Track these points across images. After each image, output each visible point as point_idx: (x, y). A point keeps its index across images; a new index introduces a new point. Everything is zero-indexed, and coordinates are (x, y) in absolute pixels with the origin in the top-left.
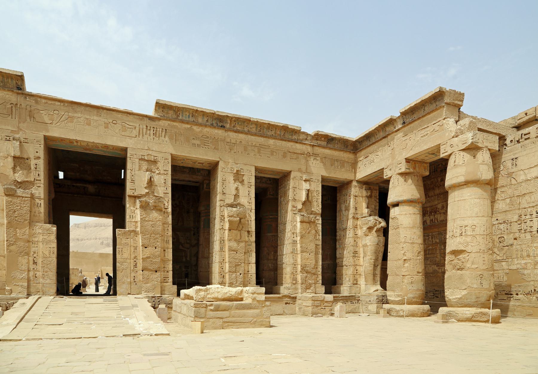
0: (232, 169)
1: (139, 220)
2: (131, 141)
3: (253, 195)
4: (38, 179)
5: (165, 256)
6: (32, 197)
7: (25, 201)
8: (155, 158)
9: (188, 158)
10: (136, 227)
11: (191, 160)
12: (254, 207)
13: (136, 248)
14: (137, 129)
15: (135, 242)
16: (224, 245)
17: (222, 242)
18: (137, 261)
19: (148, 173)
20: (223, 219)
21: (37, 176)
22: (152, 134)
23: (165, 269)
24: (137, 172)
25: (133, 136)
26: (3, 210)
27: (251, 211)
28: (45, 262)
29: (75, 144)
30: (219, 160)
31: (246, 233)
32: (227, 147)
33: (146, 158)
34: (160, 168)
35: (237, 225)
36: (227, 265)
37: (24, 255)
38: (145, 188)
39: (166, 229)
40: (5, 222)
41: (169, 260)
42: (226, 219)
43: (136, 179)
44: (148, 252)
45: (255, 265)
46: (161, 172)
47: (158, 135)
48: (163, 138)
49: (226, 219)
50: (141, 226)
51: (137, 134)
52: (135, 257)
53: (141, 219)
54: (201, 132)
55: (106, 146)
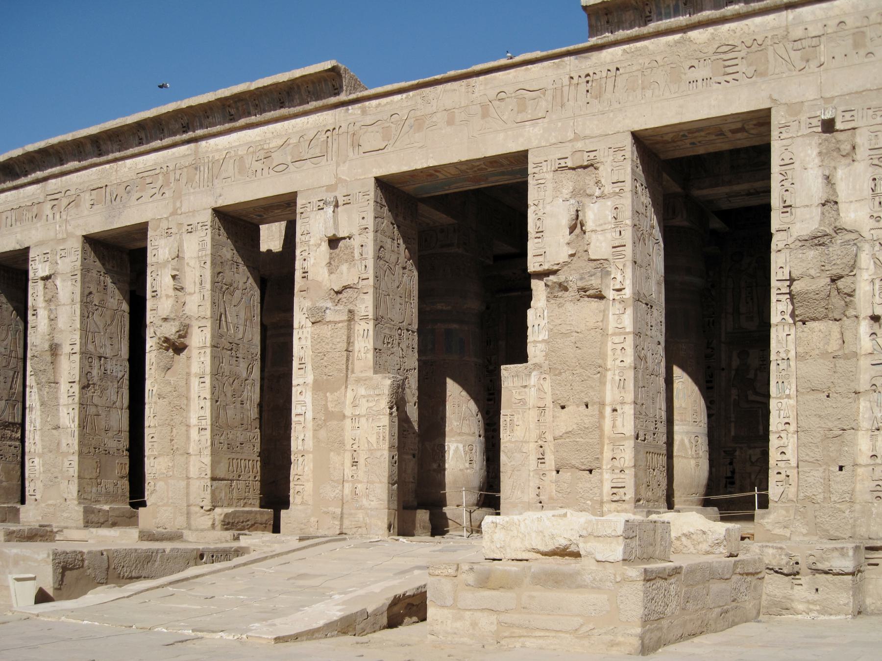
4: (365, 276)
8: (592, 155)
13: (542, 409)
32: (796, 56)
34: (603, 181)
39: (620, 347)
46: (606, 192)
54: (713, 38)
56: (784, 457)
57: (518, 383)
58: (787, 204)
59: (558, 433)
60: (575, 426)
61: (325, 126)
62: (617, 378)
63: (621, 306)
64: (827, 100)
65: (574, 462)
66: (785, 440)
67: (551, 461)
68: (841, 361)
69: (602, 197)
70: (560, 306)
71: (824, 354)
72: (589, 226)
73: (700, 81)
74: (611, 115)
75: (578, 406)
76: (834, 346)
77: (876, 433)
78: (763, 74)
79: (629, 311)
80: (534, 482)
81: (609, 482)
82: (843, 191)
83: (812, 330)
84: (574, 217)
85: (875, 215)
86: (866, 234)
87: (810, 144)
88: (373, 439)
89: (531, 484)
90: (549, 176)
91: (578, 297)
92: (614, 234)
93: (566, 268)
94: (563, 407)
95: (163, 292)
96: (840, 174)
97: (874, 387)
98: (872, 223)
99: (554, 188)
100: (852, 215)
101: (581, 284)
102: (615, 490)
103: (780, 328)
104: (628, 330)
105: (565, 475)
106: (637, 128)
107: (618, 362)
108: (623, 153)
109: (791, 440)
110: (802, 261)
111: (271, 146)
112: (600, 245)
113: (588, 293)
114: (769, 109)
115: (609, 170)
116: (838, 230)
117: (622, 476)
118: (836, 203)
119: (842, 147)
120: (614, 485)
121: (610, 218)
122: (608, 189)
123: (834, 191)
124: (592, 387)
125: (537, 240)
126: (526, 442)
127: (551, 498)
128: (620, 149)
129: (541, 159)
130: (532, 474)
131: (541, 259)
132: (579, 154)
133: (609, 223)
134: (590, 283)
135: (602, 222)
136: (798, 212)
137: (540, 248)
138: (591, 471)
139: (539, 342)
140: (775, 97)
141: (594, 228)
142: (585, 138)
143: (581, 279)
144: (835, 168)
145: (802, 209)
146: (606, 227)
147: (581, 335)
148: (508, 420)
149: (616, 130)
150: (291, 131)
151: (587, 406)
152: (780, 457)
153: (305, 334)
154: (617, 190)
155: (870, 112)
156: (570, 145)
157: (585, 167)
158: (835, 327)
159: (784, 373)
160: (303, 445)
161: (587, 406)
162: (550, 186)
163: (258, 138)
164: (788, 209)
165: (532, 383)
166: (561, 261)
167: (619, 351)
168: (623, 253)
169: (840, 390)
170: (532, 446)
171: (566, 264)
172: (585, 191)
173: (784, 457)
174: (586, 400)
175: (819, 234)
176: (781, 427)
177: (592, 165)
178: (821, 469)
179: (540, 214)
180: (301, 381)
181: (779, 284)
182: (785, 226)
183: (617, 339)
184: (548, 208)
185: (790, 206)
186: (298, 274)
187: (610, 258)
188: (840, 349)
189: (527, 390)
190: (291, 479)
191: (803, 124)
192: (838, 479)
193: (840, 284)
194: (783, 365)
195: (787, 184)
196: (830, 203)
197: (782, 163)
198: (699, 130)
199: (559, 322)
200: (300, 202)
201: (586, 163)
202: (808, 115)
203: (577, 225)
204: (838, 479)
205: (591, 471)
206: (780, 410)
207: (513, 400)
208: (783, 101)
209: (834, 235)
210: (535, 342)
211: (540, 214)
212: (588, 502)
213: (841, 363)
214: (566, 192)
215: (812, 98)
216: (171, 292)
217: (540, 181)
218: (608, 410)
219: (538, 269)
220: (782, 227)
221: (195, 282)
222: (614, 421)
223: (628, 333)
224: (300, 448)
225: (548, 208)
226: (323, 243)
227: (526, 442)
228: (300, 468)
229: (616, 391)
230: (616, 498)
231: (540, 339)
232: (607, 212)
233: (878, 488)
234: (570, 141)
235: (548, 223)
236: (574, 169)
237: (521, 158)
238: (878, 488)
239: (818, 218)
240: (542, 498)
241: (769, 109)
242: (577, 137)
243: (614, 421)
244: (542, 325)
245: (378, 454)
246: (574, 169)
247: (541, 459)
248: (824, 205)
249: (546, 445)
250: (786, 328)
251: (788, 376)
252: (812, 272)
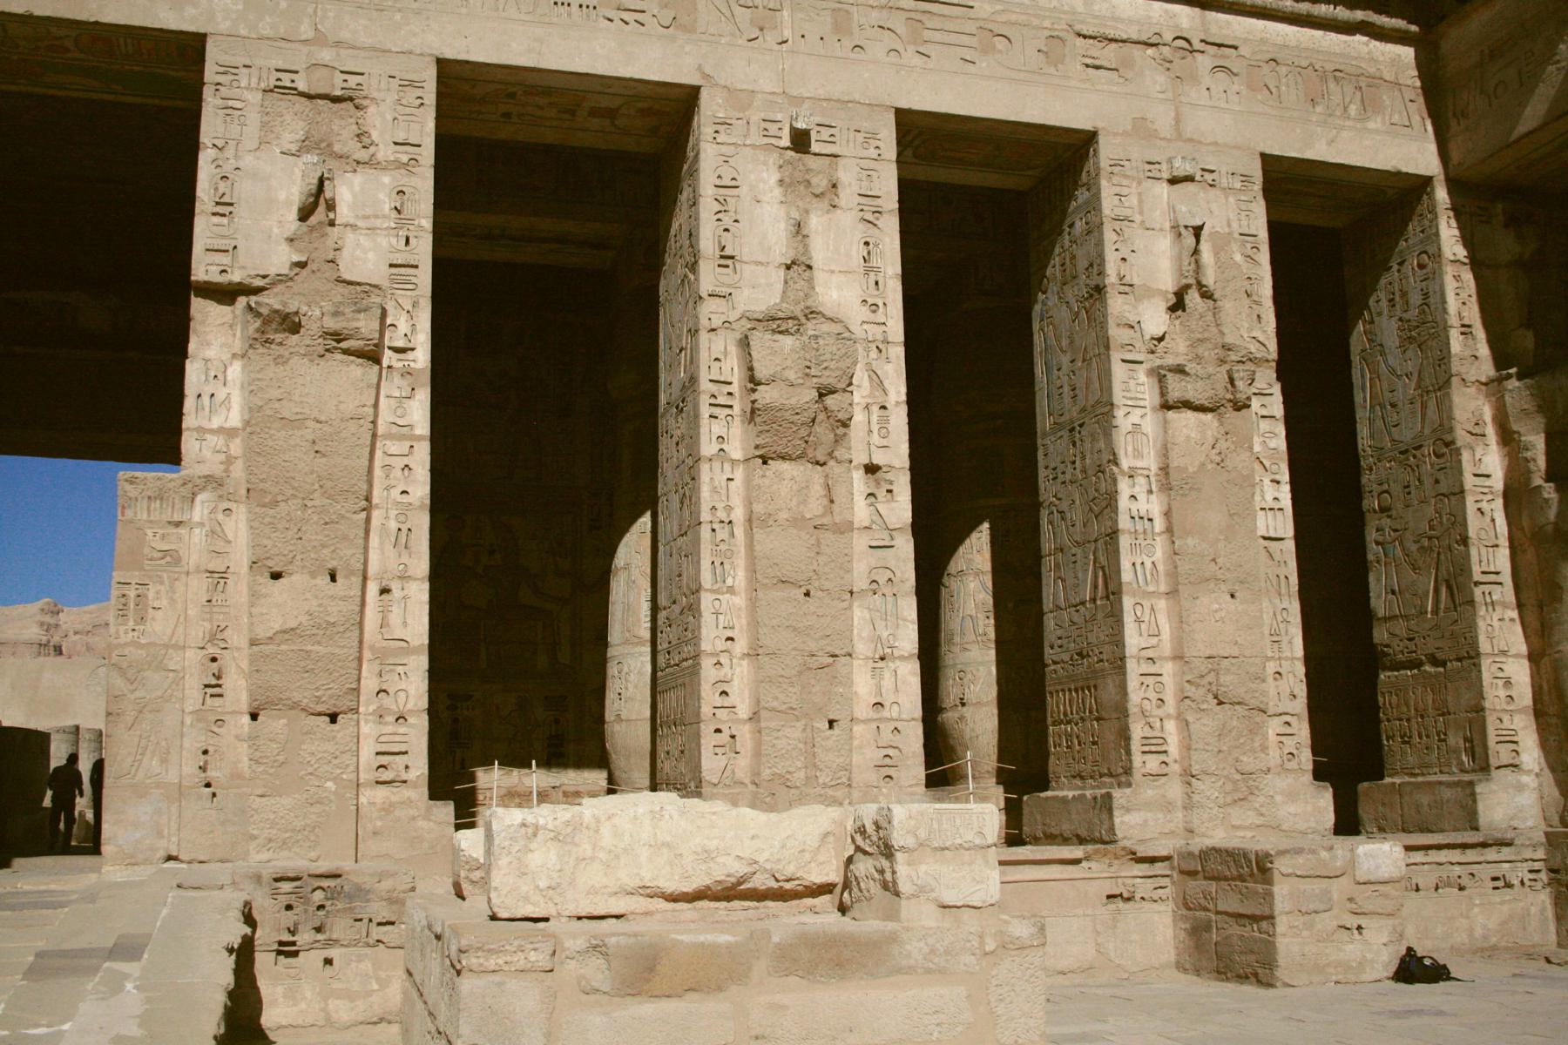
13: (219, 577)
15: (220, 545)
31: (858, 476)
34: (375, 135)
43: (245, 200)
46: (380, 156)
56: (727, 702)
57: (162, 513)
58: (727, 252)
59: (262, 632)
60: (304, 619)
62: (393, 525)
63: (405, 383)
64: (798, 100)
65: (297, 696)
66: (726, 669)
67: (238, 690)
68: (829, 535)
69: (371, 163)
70: (280, 360)
71: (797, 521)
72: (344, 213)
73: (575, 8)
74: (398, 17)
75: (313, 575)
76: (815, 507)
77: (881, 664)
78: (690, 29)
79: (423, 397)
80: (193, 741)
81: (371, 741)
82: (819, 254)
83: (779, 476)
84: (314, 188)
85: (870, 301)
86: (858, 331)
87: (765, 163)
89: (187, 743)
90: (255, 98)
91: (321, 350)
92: (394, 241)
93: (281, 287)
94: (276, 576)
96: (815, 222)
97: (874, 586)
98: (865, 314)
99: (264, 125)
100: (835, 294)
101: (331, 324)
102: (384, 760)
103: (716, 465)
104: (418, 432)
105: (274, 724)
106: (450, 54)
107: (395, 493)
108: (419, 93)
109: (738, 670)
110: (774, 353)
112: (365, 256)
113: (344, 345)
114: (699, 88)
115: (389, 117)
116: (811, 313)
117: (402, 730)
118: (810, 267)
119: (814, 181)
121: (387, 207)
122: (385, 152)
123: (806, 247)
124: (345, 538)
125: (216, 219)
126: (176, 647)
127: (240, 776)
128: (412, 84)
129: (240, 61)
130: (188, 720)
131: (225, 259)
132: (320, 73)
133: (384, 217)
134: (355, 324)
135: (369, 211)
136: (747, 270)
137: (223, 237)
138: (333, 718)
139: (212, 431)
140: (707, 70)
141: (352, 221)
142: (338, 44)
143: (336, 314)
144: (807, 212)
145: (753, 267)
146: (378, 223)
147: (326, 428)
148: (132, 594)
149: (406, 47)
151: (333, 578)
152: (719, 701)
154: (405, 159)
155: (860, 137)
156: (305, 49)
157: (336, 100)
158: (817, 474)
159: (723, 547)
161: (333, 578)
162: (254, 118)
164: (729, 262)
165: (196, 517)
166: (272, 271)
167: (397, 473)
168: (414, 280)
169: (827, 585)
170: (193, 657)
171: (281, 279)
172: (329, 145)
173: (727, 702)
174: (332, 564)
175: (781, 315)
176: (721, 645)
177: (351, 99)
178: (799, 725)
179: (228, 168)
181: (713, 388)
182: (724, 290)
183: (394, 447)
184: (248, 161)
185: (732, 257)
187: (385, 283)
188: (823, 515)
189: (182, 531)
191: (753, 129)
192: (830, 743)
193: (830, 401)
194: (722, 533)
195: (727, 220)
196: (798, 265)
197: (718, 182)
198: (547, 91)
199: (276, 394)
201: (338, 93)
202: (763, 115)
203: (316, 203)
204: (830, 743)
205: (333, 718)
206: (717, 613)
207: (146, 551)
208: (722, 82)
209: (803, 320)
210: (200, 429)
211: (228, 168)
212: (329, 784)
213: (827, 538)
214: (291, 134)
215: (769, 89)
217: (230, 103)
218: (373, 589)
219: (215, 277)
220: (718, 290)
222: (385, 612)
223: (420, 438)
225: (248, 161)
227: (176, 647)
229: (391, 552)
230: (386, 775)
231: (216, 423)
232: (381, 196)
233: (888, 761)
234: (305, 41)
235: (244, 190)
236: (310, 97)
238: (888, 761)
239: (780, 286)
240: (212, 774)
241: (699, 88)
242: (320, 40)
243: (385, 612)
244: (221, 394)
246: (310, 97)
247: (214, 687)
248: (788, 267)
249: (226, 659)
250: (727, 466)
251: (730, 554)
252: (791, 375)
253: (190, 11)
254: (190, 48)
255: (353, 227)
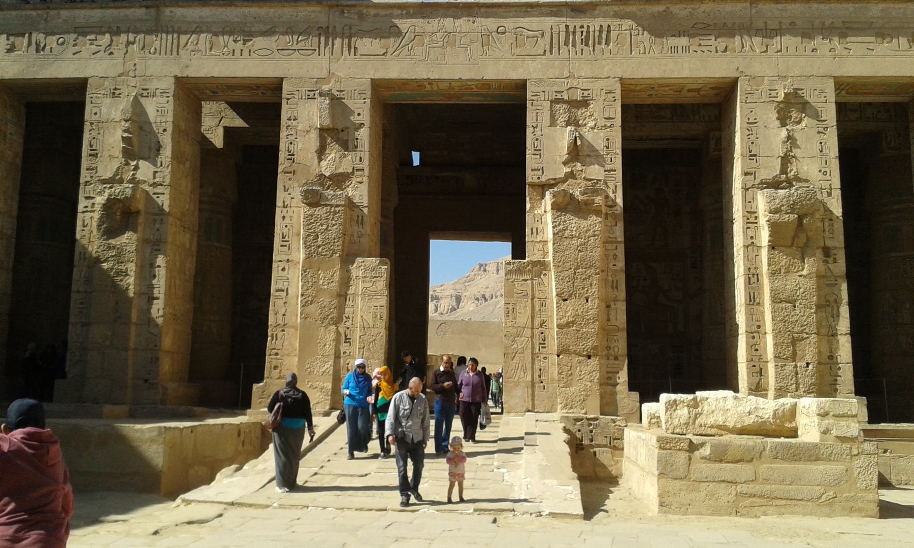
0: (774, 93)
1: (551, 236)
2: (535, 64)
3: (833, 150)
4: (360, 166)
5: (609, 320)
6: (350, 204)
7: (335, 213)
8: (586, 93)
9: (661, 82)
10: (545, 254)
11: (669, 85)
12: (836, 182)
14: (548, 35)
15: (542, 288)
16: (760, 288)
17: (754, 280)
18: (546, 332)
19: (569, 128)
20: (752, 220)
21: (358, 162)
22: (578, 41)
23: (611, 352)
24: (546, 131)
25: (539, 53)
26: (299, 235)
27: (829, 194)
28: (366, 337)
29: (428, 88)
30: (736, 75)
33: (566, 97)
35: (792, 237)
36: (770, 340)
37: (329, 324)
38: (565, 163)
39: (612, 253)
40: (302, 256)
41: (618, 330)
42: (763, 221)
43: (547, 147)
44: (571, 307)
45: (849, 338)
47: (591, 42)
48: (603, 46)
49: (763, 221)
50: (555, 252)
51: (548, 47)
52: (543, 323)
53: (554, 234)
55: (486, 84)
61: (317, 23)
62: (610, 278)
79: (621, 225)
88: (369, 318)
95: (106, 154)
106: (626, 75)
107: (611, 265)
108: (613, 95)
111: (253, 29)
120: (609, 370)
127: (553, 380)
150: (276, 20)
153: (290, 213)
160: (284, 320)
163: (236, 19)
180: (284, 257)
186: (282, 156)
190: (268, 352)
200: (286, 87)
205: (589, 357)
216: (118, 153)
221: (150, 148)
223: (620, 242)
224: (280, 322)
226: (313, 131)
228: (279, 342)
237: (522, 86)
245: (374, 331)
253: (521, 70)
254: (522, 86)
255: (589, 156)
